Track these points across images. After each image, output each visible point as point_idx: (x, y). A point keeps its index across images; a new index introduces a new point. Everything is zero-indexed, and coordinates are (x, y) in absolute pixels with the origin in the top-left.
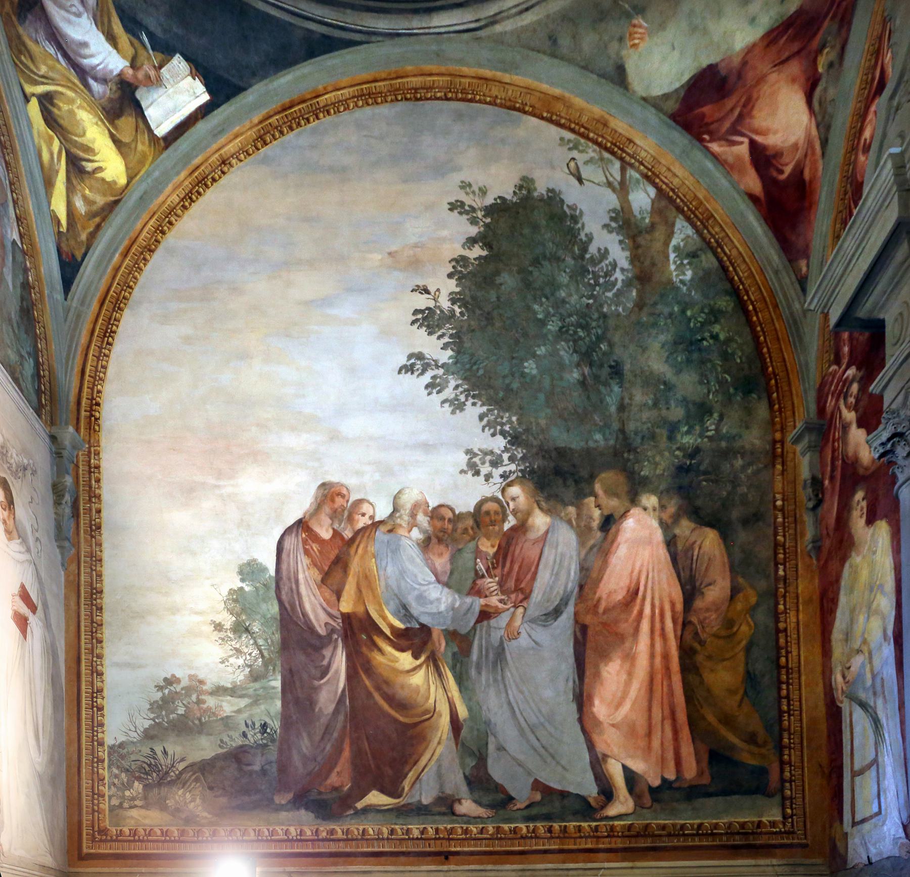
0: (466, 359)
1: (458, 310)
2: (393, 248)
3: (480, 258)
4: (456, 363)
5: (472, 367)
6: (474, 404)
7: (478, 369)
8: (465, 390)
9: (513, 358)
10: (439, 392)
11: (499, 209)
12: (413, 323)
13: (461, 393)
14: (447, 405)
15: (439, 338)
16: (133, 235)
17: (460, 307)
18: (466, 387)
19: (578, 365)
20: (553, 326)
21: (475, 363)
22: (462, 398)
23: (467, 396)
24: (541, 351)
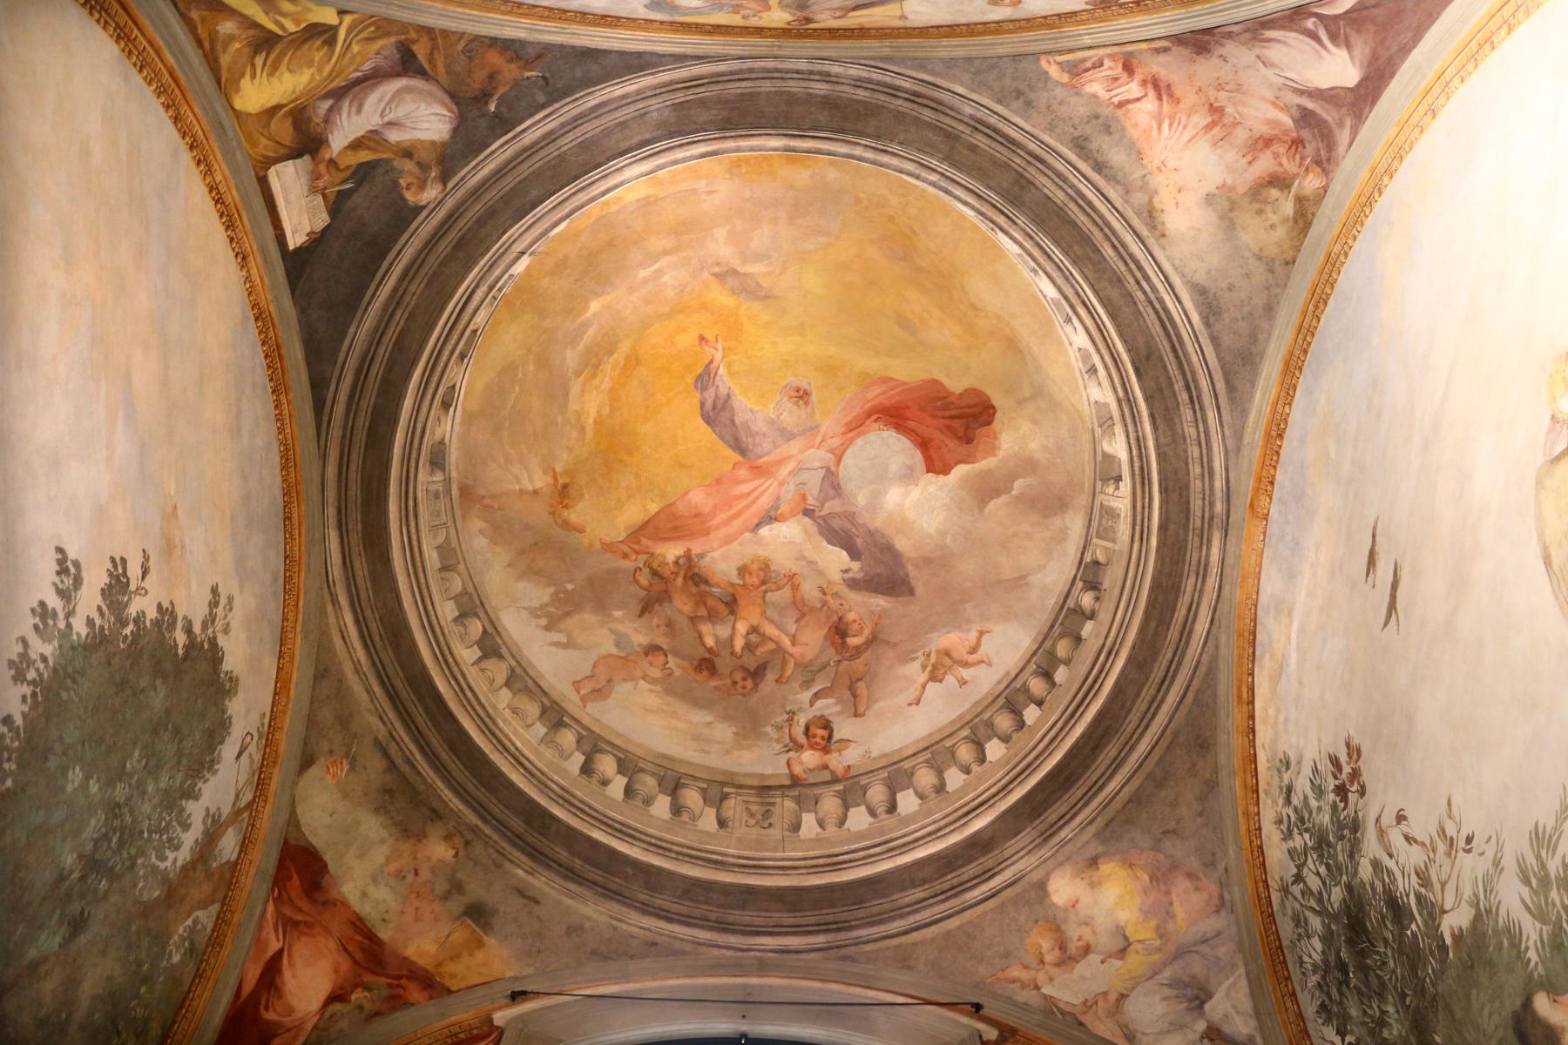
0: (78, 663)
1: (128, 631)
2: (180, 512)
3: (176, 646)
4: (73, 648)
5: (70, 677)
6: (24, 698)
7: (67, 689)
8: (40, 675)
9: (83, 743)
10: (36, 627)
11: (215, 655)
12: (113, 560)
13: (37, 670)
14: (19, 648)
15: (99, 609)
16: (189, 95)
17: (132, 632)
18: (46, 675)
19: (81, 857)
20: (120, 792)
21: (74, 681)
22: (31, 675)
23: (33, 683)
24: (94, 787)
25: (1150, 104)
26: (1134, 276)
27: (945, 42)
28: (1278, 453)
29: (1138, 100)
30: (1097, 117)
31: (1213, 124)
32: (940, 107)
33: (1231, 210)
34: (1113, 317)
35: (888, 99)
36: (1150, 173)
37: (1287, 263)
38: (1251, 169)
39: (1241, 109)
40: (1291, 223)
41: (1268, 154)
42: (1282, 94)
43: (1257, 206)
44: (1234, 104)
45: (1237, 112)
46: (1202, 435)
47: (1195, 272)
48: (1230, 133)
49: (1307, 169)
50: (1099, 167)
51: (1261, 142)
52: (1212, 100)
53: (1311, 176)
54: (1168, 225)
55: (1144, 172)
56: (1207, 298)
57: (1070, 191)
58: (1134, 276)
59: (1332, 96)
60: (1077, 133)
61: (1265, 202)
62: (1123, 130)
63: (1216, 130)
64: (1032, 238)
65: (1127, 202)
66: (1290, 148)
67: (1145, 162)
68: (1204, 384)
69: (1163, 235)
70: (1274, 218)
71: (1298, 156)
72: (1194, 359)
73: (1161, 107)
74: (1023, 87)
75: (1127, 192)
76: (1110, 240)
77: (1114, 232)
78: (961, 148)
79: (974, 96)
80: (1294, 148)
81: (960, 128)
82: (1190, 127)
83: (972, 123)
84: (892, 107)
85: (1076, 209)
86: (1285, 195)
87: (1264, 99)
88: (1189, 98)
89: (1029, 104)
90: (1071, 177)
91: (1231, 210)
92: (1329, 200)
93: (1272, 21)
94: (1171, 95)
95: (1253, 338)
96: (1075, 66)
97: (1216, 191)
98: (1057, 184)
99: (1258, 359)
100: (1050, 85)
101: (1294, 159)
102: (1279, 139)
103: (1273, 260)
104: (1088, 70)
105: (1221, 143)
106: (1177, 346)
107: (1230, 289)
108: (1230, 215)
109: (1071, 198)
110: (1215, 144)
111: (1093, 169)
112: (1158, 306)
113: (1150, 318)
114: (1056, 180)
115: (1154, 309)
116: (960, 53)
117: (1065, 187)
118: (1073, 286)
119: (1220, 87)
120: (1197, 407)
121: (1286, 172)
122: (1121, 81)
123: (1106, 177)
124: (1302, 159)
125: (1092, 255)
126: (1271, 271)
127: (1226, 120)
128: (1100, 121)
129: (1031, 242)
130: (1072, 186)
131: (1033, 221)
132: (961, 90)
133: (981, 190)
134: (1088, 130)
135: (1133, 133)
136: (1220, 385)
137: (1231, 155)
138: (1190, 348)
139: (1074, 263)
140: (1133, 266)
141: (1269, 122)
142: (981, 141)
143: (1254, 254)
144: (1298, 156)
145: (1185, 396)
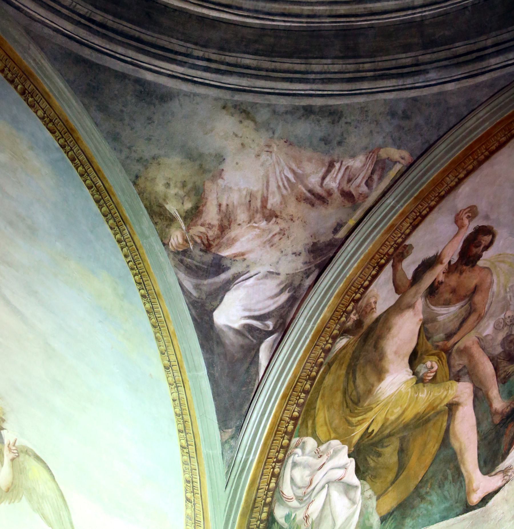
25: (314, 181)
26: (216, 61)
27: (487, 126)
28: (12, 82)
29: (323, 178)
30: (340, 143)
31: (264, 206)
32: (455, 61)
33: (201, 166)
34: (202, 18)
35: (500, 38)
36: (272, 138)
37: (137, 177)
38: (215, 203)
39: (257, 231)
40: (161, 201)
41: (216, 222)
42: (245, 264)
43: (190, 186)
44: (264, 230)
45: (258, 228)
46: (58, 8)
47: (181, 106)
48: (249, 209)
49: (186, 241)
50: (308, 111)
51: (226, 223)
52: (279, 220)
53: (181, 240)
54: (227, 117)
55: (276, 135)
56: (157, 98)
57: (313, 76)
58: (216, 61)
59: (218, 296)
60: (343, 120)
61: (188, 194)
62: (315, 150)
63: (258, 204)
64: (308, 16)
65: (269, 105)
66: (208, 240)
67: (282, 141)
68: (97, 41)
69: (224, 107)
70: (172, 191)
71: (198, 240)
72: (120, 49)
73: (305, 186)
74: (405, 123)
75: (274, 112)
76: (255, 69)
77: (258, 77)
78: (416, 40)
79: (436, 89)
80: (206, 242)
81: (428, 56)
82: (276, 189)
83: (422, 67)
84: (494, 34)
85: (297, 67)
86: (182, 211)
87: (250, 251)
88: (293, 208)
89: (393, 114)
90: (321, 87)
91: (201, 166)
92: (158, 246)
93: (292, 306)
94: (306, 200)
95: (103, 108)
96: (383, 169)
97: (221, 167)
98: (325, 73)
99: (86, 101)
100: (389, 140)
101: (199, 237)
102: (218, 237)
103: (146, 167)
104: (373, 173)
105: (248, 199)
106: (140, 45)
107: (149, 119)
108: (198, 162)
109: (307, 72)
110: (251, 195)
111: (311, 106)
112: (180, 58)
113: (176, 44)
114: (329, 76)
115: (181, 54)
116: (471, 123)
117: (318, 76)
118: (248, 10)
119: (282, 232)
120: (83, 21)
121: (195, 225)
122: (345, 182)
123: (296, 109)
124: (195, 243)
125: (257, 46)
126: (139, 160)
127: (259, 216)
128: (335, 142)
129: (306, 13)
130: (314, 81)
131: (319, 30)
132: (450, 87)
133: (375, 21)
134: (338, 130)
135: (308, 153)
136: (86, 53)
137: (235, 198)
138: (131, 53)
139: (263, 28)
140: (223, 67)
141: (233, 241)
142: (405, 58)
143: (159, 157)
144: (198, 240)
145: (98, 18)
